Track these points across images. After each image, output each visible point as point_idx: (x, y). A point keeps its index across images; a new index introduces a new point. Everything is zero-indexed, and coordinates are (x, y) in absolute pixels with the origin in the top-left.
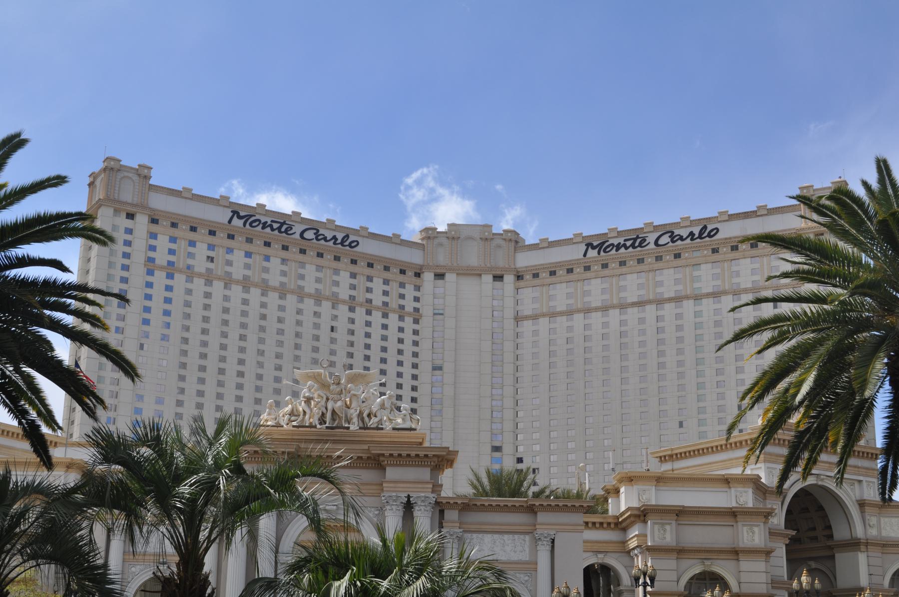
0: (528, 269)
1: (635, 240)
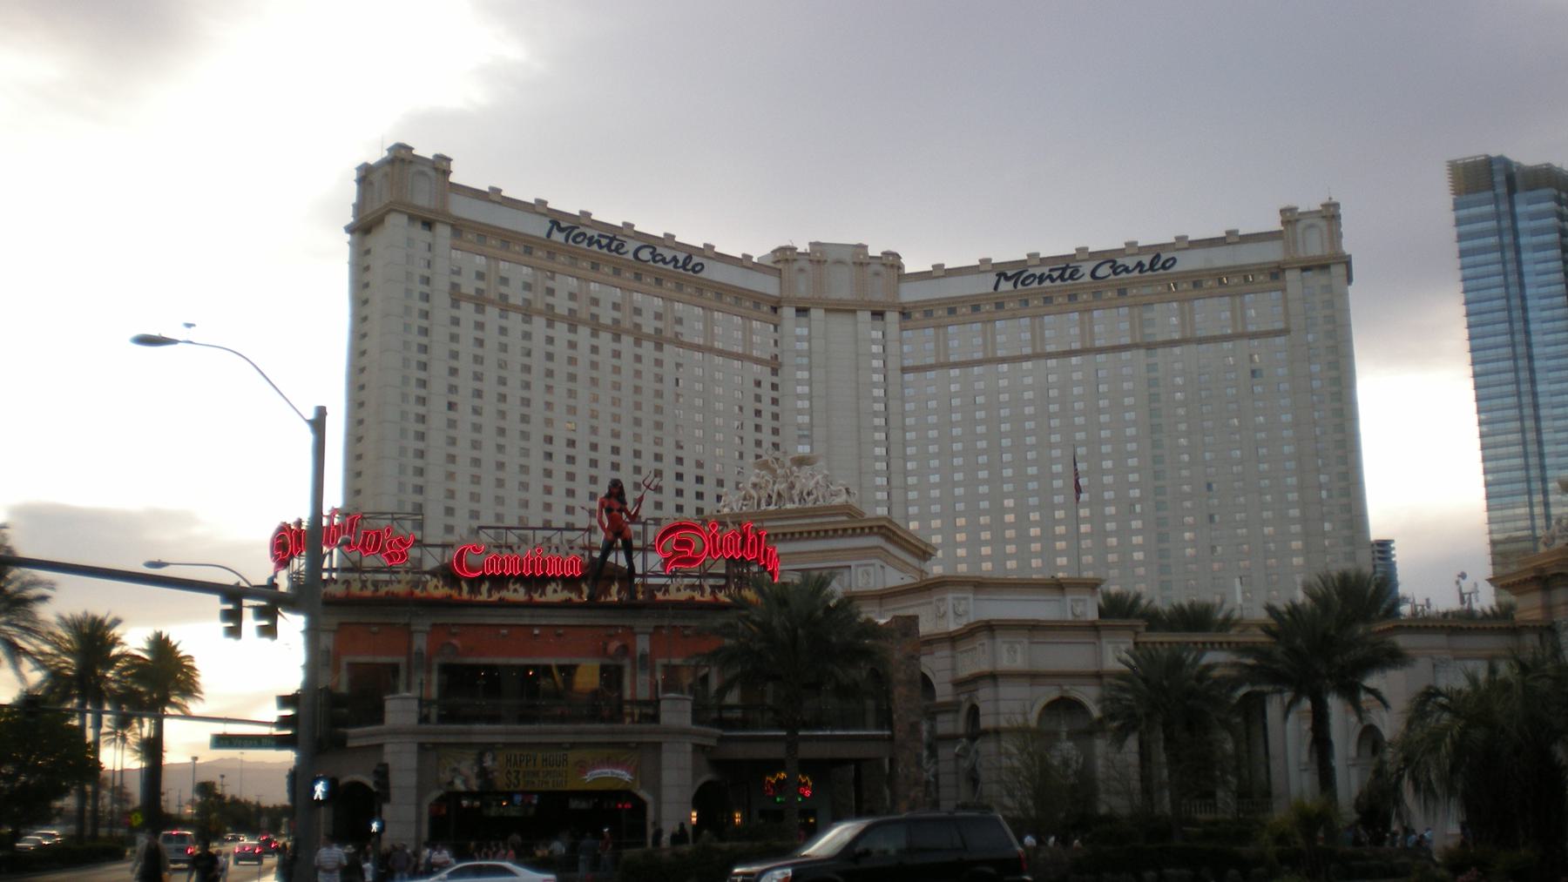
0: (917, 305)
1: (1064, 270)
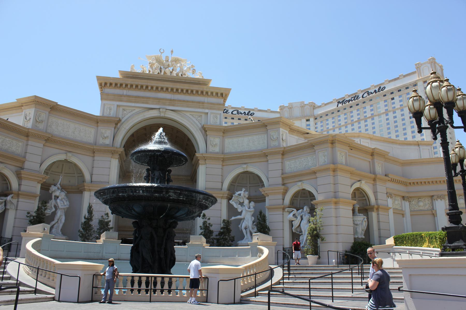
1: (355, 97)
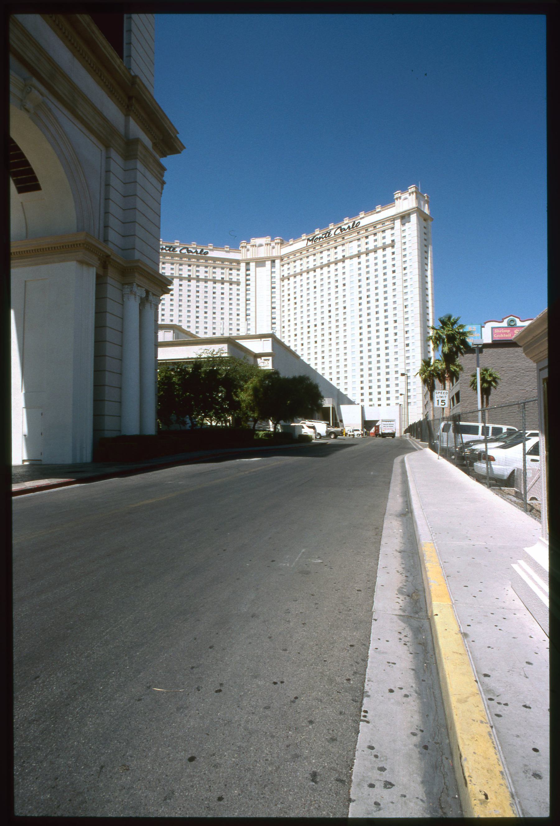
1: (326, 234)
